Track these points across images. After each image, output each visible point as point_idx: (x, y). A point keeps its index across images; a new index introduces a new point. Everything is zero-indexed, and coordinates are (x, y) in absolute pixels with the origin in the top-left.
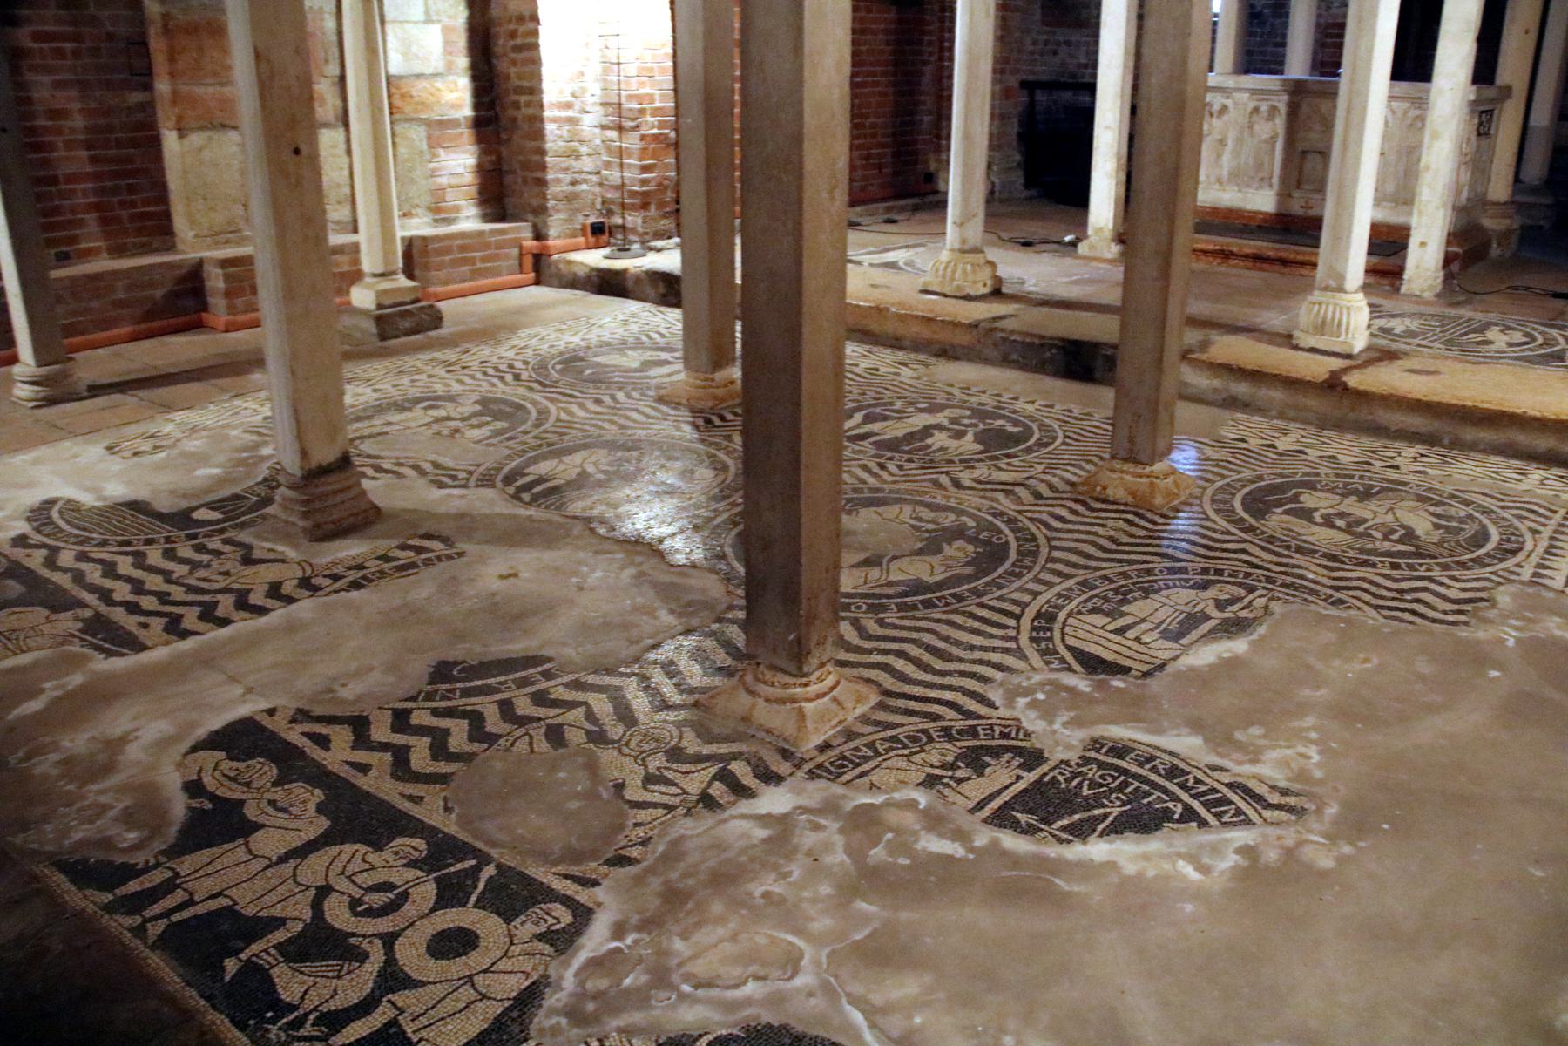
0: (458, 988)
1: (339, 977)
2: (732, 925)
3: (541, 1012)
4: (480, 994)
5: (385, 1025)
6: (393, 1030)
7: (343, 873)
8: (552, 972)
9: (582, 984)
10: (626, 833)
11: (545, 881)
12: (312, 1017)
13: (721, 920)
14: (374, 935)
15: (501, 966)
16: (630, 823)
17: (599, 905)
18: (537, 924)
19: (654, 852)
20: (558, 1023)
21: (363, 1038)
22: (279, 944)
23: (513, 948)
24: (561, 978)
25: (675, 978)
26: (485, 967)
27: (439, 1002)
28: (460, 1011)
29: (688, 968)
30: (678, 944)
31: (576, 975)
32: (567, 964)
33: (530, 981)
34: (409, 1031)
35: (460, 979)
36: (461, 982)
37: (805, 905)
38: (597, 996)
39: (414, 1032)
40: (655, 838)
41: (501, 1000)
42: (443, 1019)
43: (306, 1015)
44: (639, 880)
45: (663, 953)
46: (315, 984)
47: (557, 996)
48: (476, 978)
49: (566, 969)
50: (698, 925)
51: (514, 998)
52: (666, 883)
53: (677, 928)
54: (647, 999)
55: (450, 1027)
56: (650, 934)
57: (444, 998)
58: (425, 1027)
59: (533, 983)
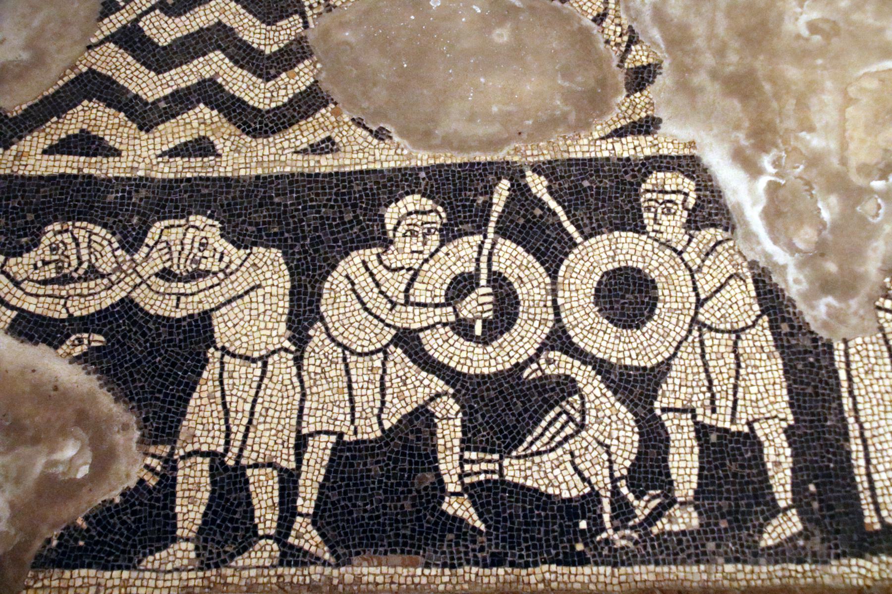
0: (702, 343)
1: (582, 426)
2: (829, 84)
3: (801, 306)
4: (729, 332)
5: (698, 438)
6: (713, 438)
7: (394, 305)
8: (751, 256)
9: (792, 248)
10: (601, 39)
11: (606, 154)
12: (624, 491)
13: (813, 87)
14: (539, 351)
15: (706, 287)
16: (587, 21)
17: (692, 144)
18: (669, 212)
19: (654, 43)
20: (828, 306)
21: (701, 469)
22: (462, 441)
23: (685, 256)
24: (768, 256)
25: (857, 180)
26: (693, 299)
27: (706, 371)
28: (738, 365)
29: (853, 162)
30: (815, 142)
31: (775, 241)
32: (750, 236)
33: (750, 281)
34: (727, 425)
35: (690, 332)
36: (695, 333)
37: (856, 17)
38: (821, 250)
39: (733, 421)
40: (634, 25)
41: (754, 323)
42: (736, 387)
43: (615, 492)
44: (685, 88)
45: (814, 160)
46: (572, 454)
47: (790, 278)
48: (701, 318)
49: (759, 243)
50: (802, 104)
51: (763, 312)
52: (714, 75)
53: (791, 124)
54: (863, 220)
55: (754, 390)
56: (775, 145)
57: (705, 364)
58: (734, 408)
59: (756, 282)
